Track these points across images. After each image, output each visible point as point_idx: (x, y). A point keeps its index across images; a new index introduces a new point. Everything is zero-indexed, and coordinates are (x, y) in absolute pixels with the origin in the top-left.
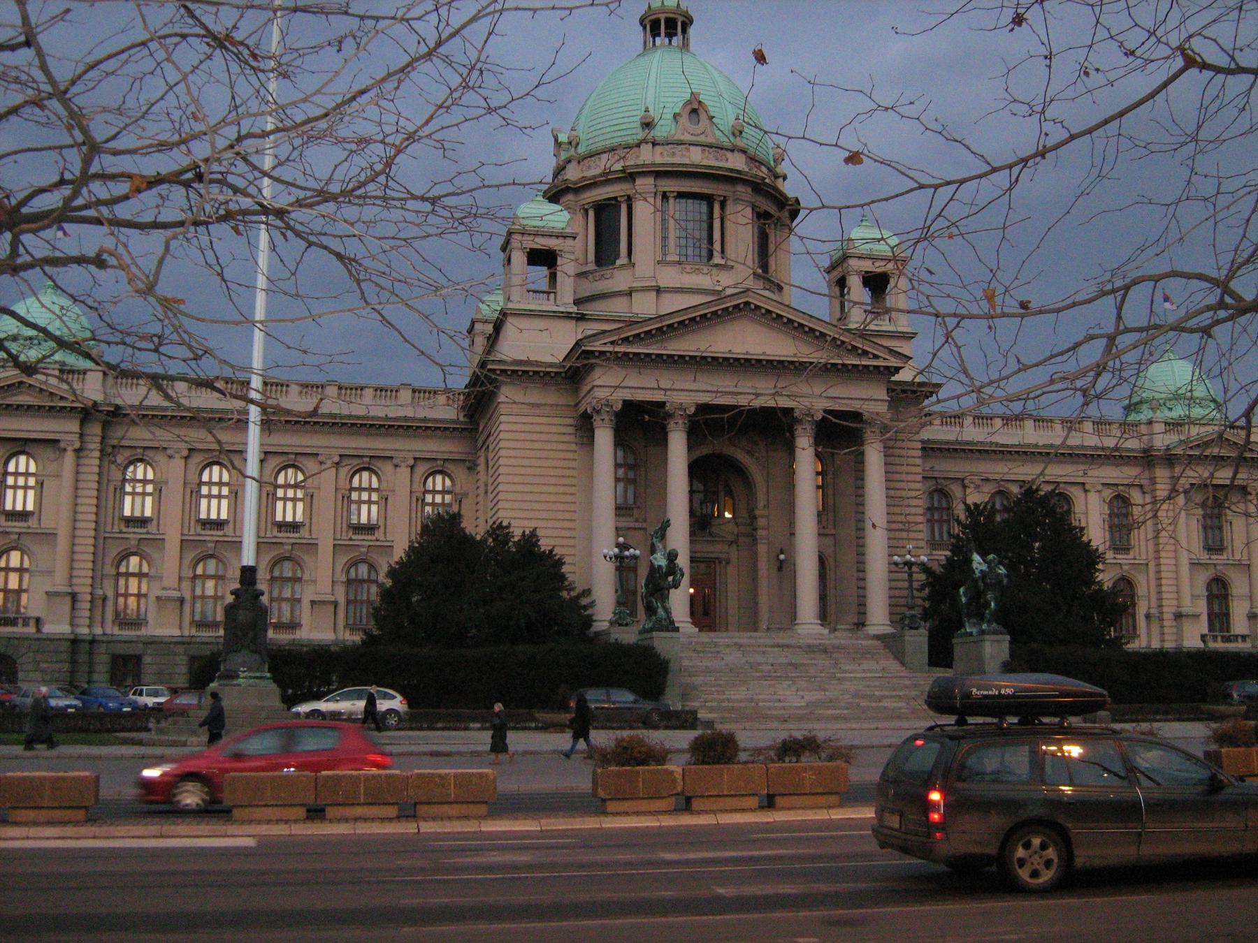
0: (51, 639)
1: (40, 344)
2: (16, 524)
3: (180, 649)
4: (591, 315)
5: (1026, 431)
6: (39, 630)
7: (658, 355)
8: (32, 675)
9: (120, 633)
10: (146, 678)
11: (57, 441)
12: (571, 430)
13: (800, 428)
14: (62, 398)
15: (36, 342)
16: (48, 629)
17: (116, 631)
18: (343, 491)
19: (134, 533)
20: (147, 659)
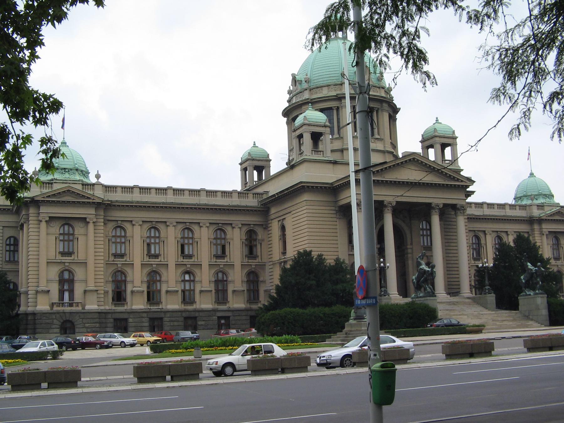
0: (90, 313)
1: (69, 171)
2: (66, 258)
3: (145, 315)
4: (339, 161)
5: (507, 211)
6: (84, 308)
7: (382, 181)
8: (81, 330)
9: (218, 307)
10: (130, 329)
11: (85, 218)
12: (334, 212)
13: (434, 211)
14: (88, 198)
15: (67, 170)
16: (88, 307)
17: (113, 308)
18: (178, 239)
19: (119, 261)
20: (130, 320)
